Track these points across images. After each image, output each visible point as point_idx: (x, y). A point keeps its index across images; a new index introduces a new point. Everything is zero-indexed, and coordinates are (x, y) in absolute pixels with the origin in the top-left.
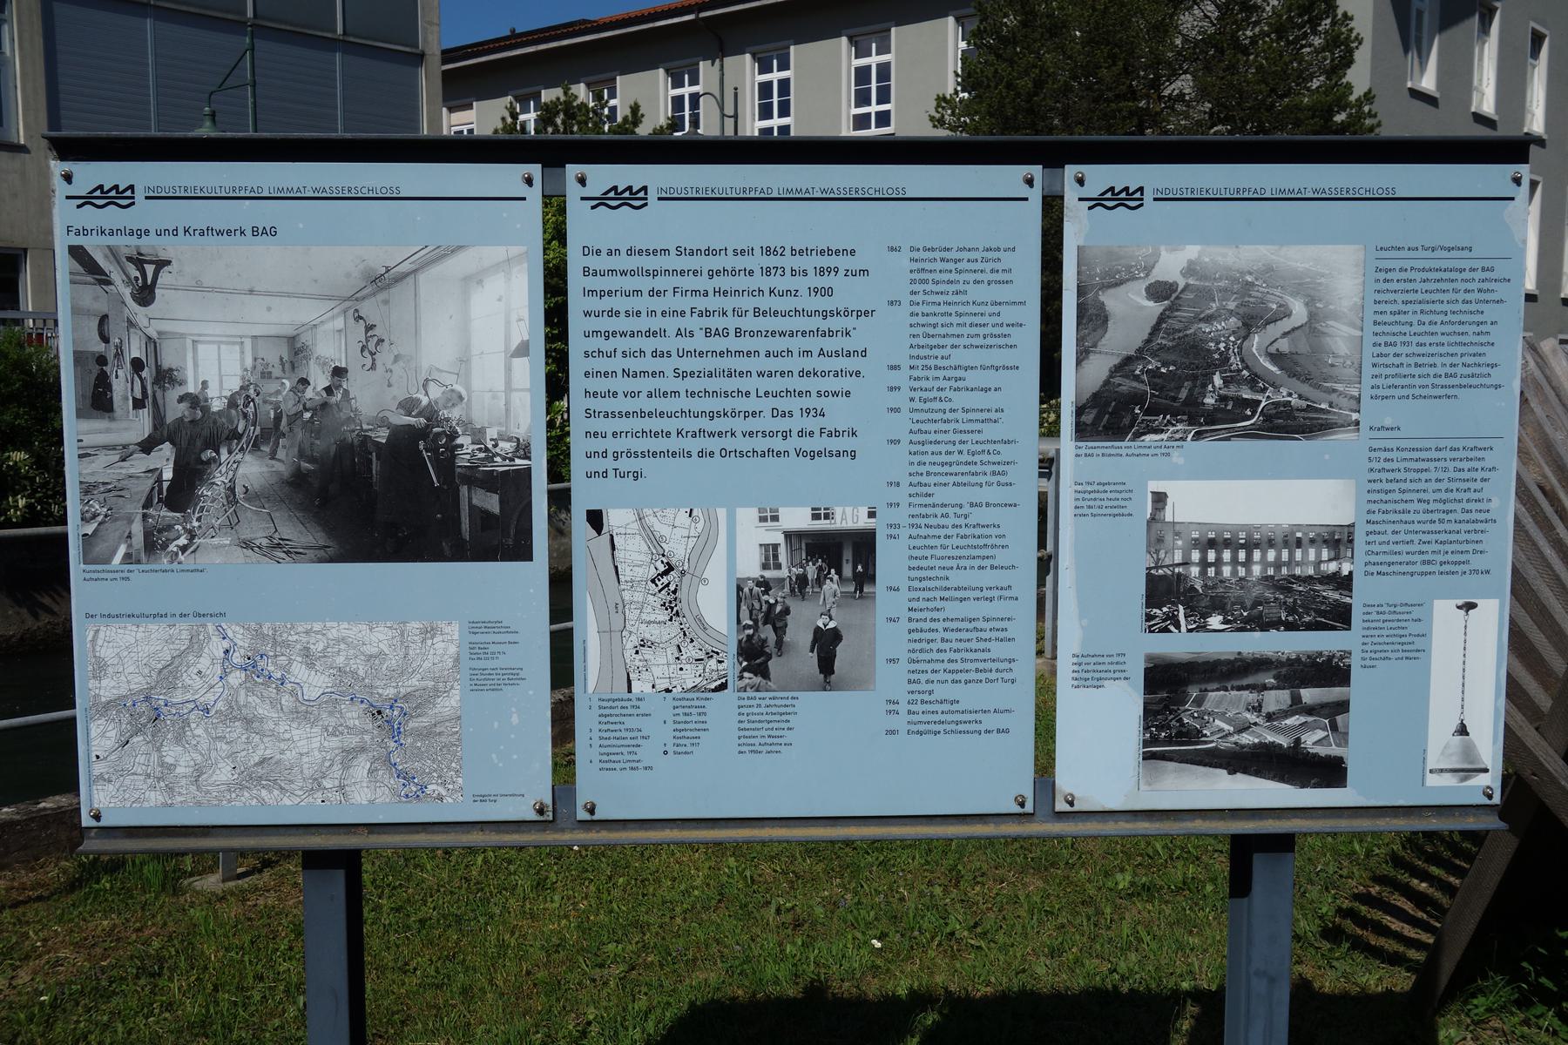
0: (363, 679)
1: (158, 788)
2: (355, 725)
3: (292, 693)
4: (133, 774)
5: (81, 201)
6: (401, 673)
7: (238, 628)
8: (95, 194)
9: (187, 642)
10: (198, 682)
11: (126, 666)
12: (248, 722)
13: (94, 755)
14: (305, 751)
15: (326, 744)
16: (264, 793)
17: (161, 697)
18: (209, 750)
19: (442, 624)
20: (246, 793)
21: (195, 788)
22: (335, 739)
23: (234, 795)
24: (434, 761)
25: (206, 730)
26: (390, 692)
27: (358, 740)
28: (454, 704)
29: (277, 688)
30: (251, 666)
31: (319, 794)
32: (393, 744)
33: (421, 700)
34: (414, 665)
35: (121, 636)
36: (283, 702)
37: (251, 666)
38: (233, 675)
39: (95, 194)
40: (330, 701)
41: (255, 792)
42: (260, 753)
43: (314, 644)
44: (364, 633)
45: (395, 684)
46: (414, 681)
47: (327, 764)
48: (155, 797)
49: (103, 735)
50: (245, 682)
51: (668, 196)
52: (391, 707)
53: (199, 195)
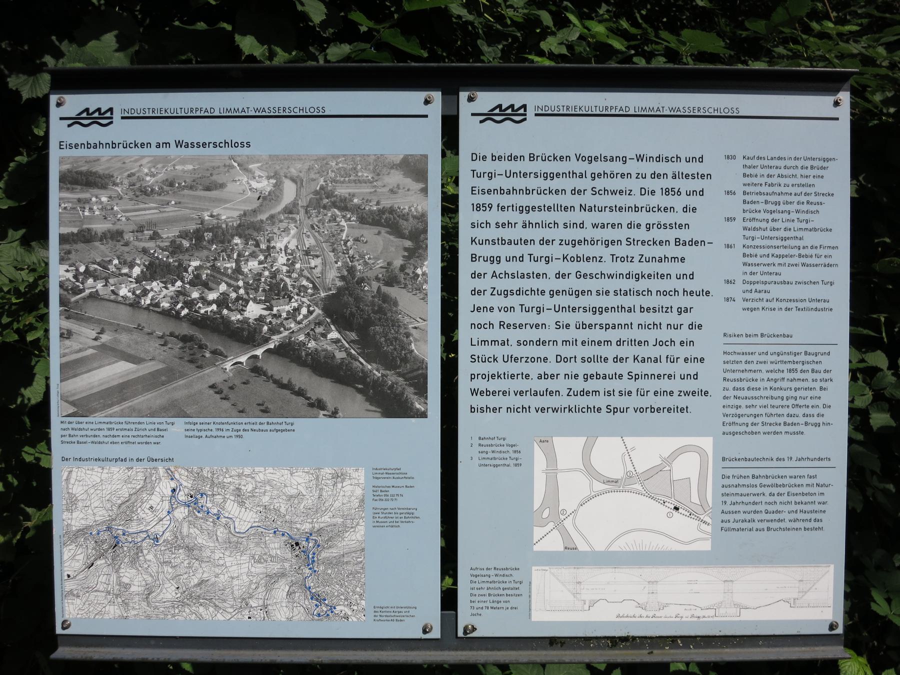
0: (284, 516)
1: (116, 603)
2: (277, 554)
3: (226, 526)
4: (96, 591)
5: (71, 122)
6: (316, 510)
7: (183, 472)
9: (142, 482)
10: (148, 517)
11: (92, 501)
12: (189, 549)
13: (66, 574)
14: (236, 575)
15: (253, 570)
16: (201, 609)
17: (120, 527)
18: (158, 573)
19: (350, 470)
20: (187, 610)
21: (145, 603)
22: (260, 565)
23: (177, 611)
24: (341, 586)
25: (156, 556)
26: (307, 527)
27: (279, 567)
28: (360, 539)
29: (213, 522)
30: (194, 502)
31: (247, 612)
32: (307, 571)
33: (333, 534)
34: (327, 504)
35: (89, 476)
36: (218, 533)
37: (194, 502)
38: (178, 510)
40: (257, 533)
41: (194, 608)
42: (199, 576)
43: (245, 486)
44: (285, 477)
45: (311, 521)
46: (326, 518)
47: (253, 587)
48: (113, 611)
49: (73, 558)
50: (188, 517)
51: (544, 112)
52: (307, 540)
53: (164, 115)
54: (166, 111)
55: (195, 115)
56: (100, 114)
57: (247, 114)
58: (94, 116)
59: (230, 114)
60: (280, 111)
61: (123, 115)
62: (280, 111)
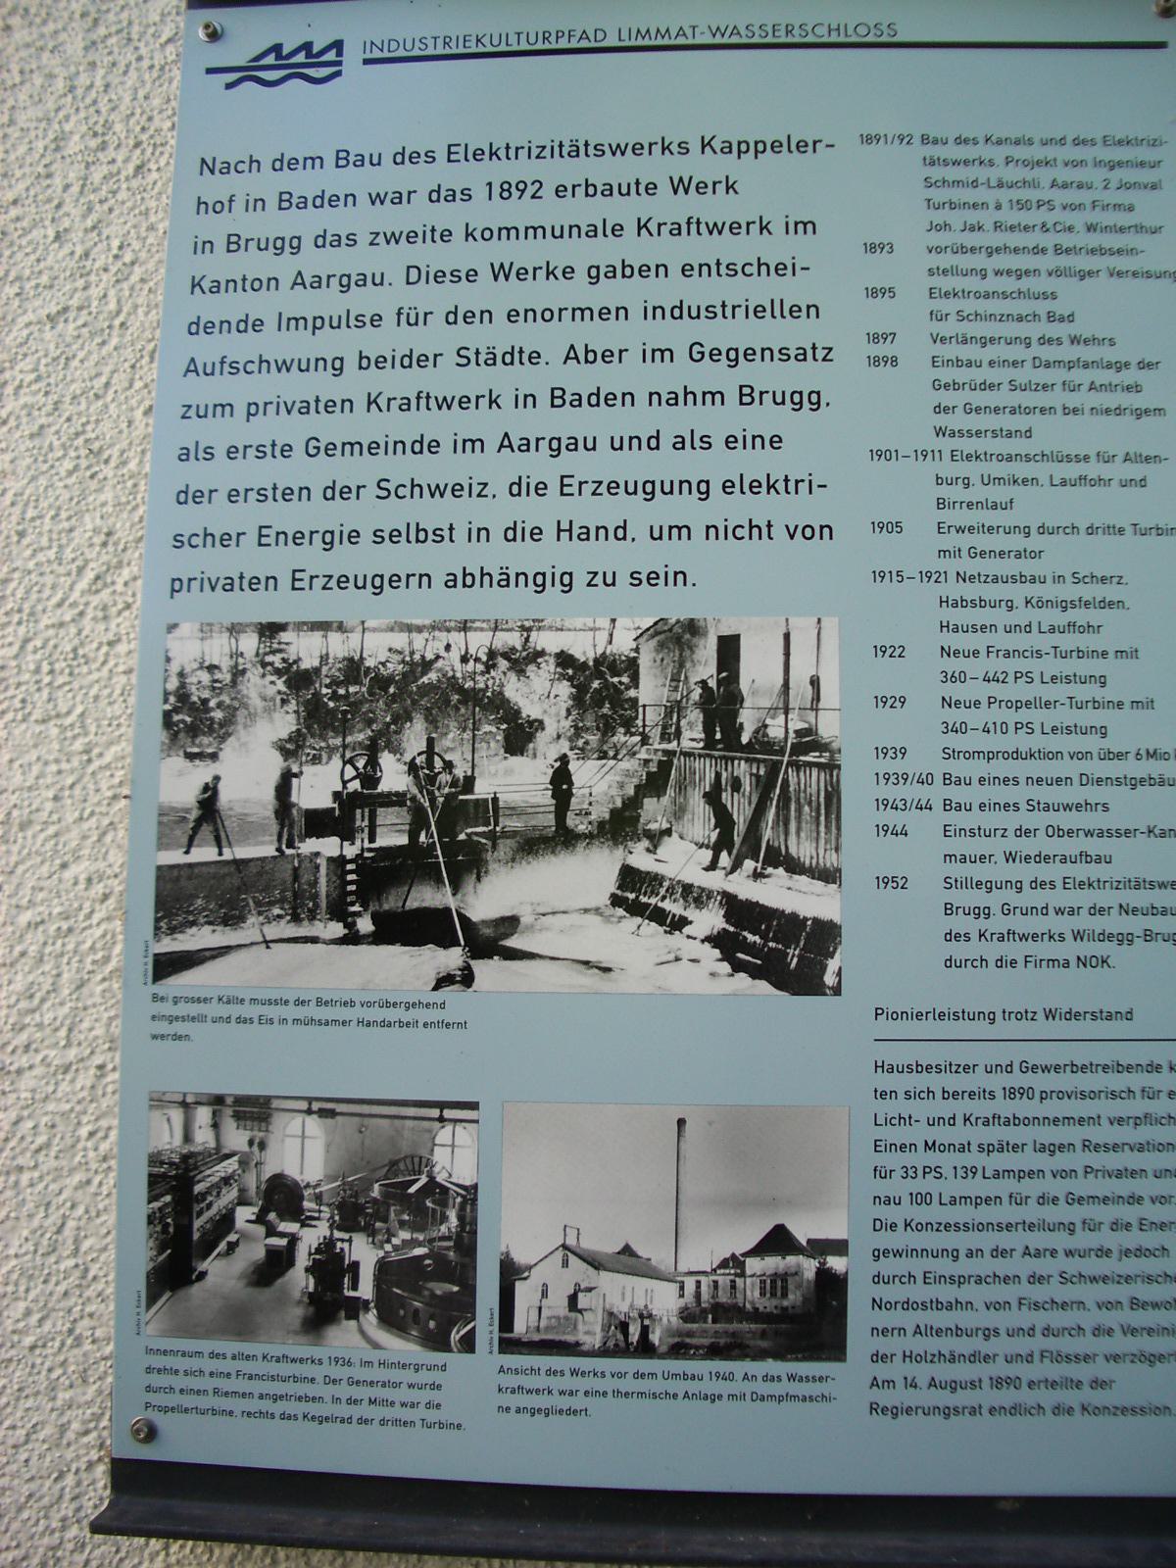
8: (262, 62)
39: (262, 62)
54: (478, 40)
55: (554, 46)
56: (309, 55)
57: (690, 41)
58: (294, 60)
59: (647, 42)
61: (368, 56)
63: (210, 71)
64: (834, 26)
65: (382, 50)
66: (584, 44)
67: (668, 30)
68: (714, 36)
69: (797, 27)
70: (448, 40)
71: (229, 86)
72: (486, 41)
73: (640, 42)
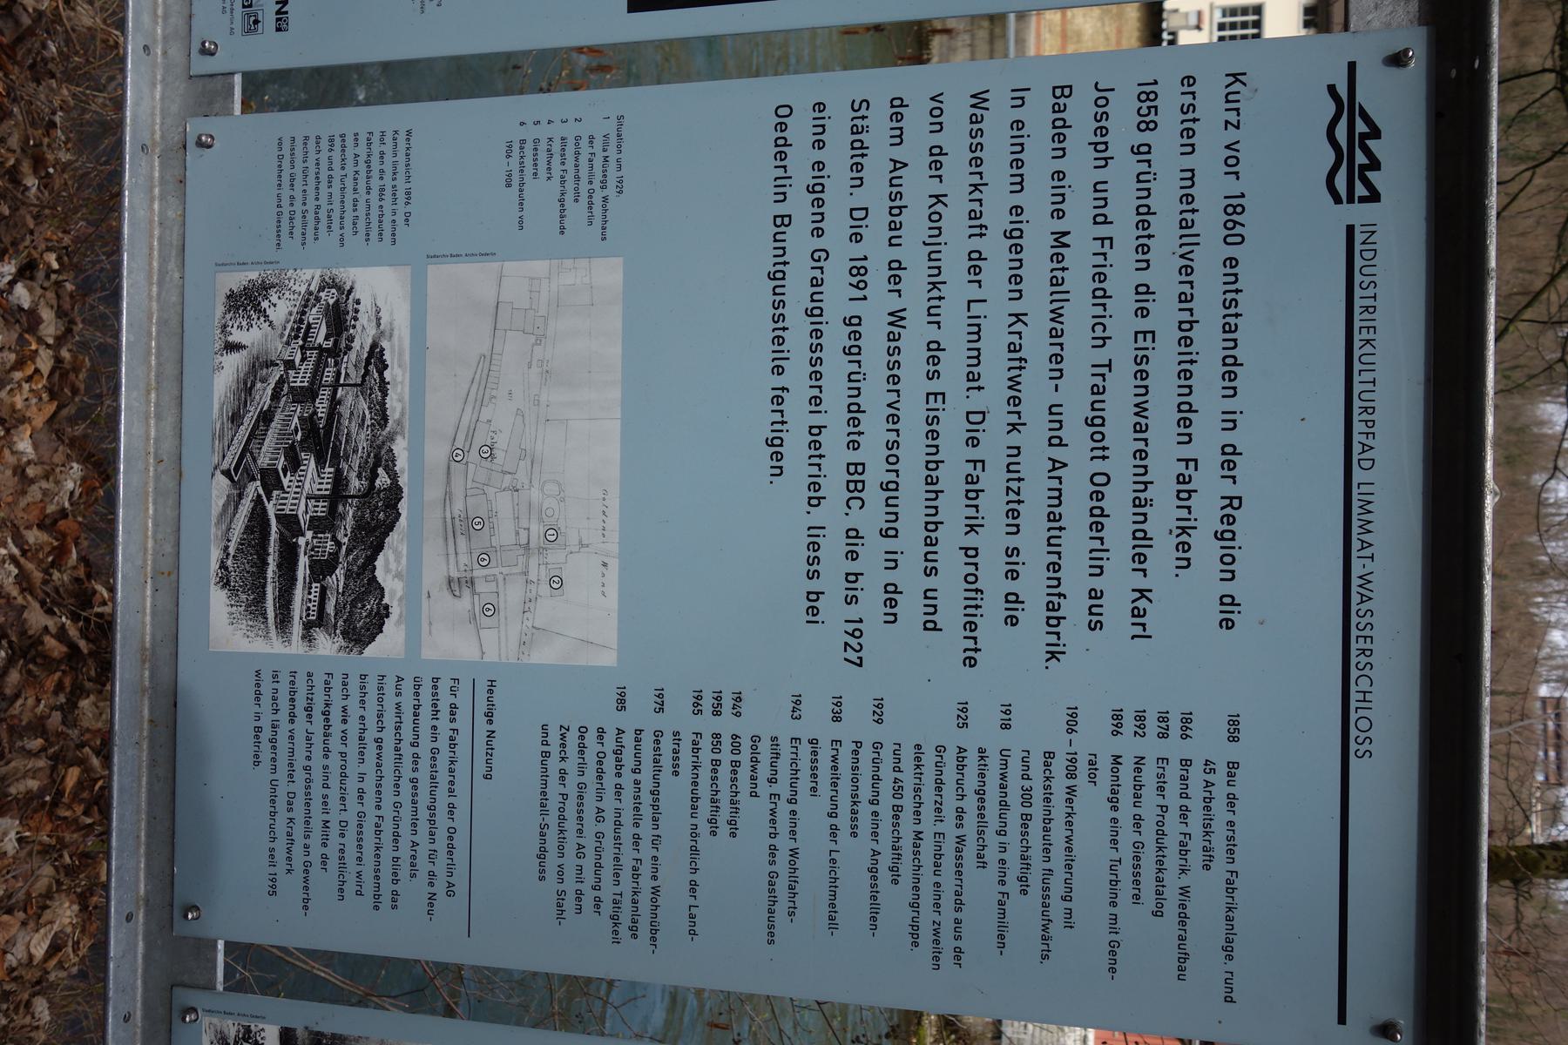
53: (1357, 337)
54: (1368, 341)
55: (1356, 418)
56: (1363, 168)
57: (1354, 554)
59: (1355, 510)
60: (1361, 640)
61: (1357, 230)
62: (1361, 640)
63: (1352, 67)
64: (1368, 697)
65: (1364, 243)
66: (1356, 448)
67: (1370, 532)
68: (1360, 577)
69: (1368, 660)
70: (1371, 310)
71: (1332, 89)
72: (1368, 349)
73: (1355, 504)
